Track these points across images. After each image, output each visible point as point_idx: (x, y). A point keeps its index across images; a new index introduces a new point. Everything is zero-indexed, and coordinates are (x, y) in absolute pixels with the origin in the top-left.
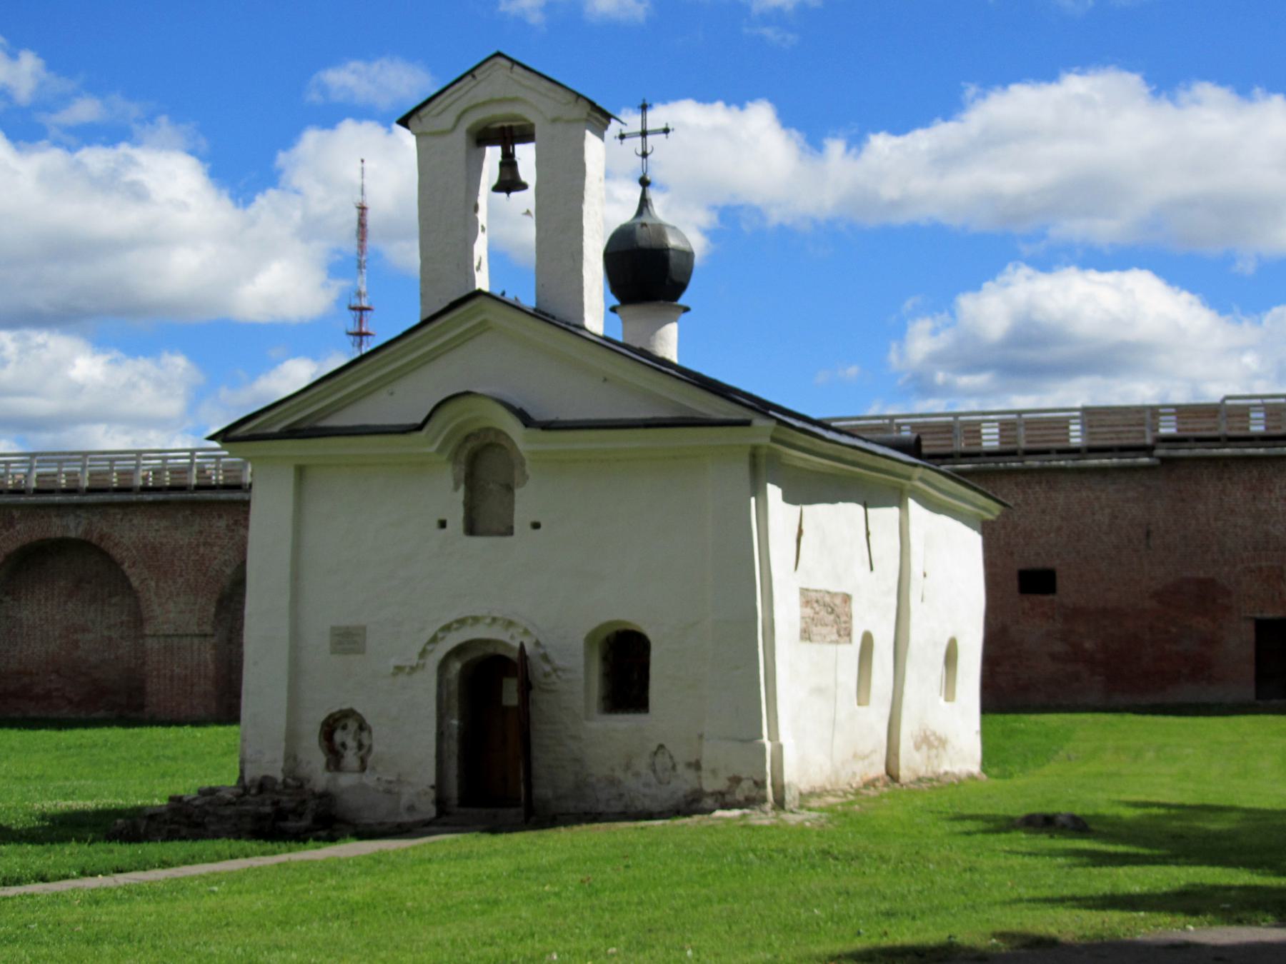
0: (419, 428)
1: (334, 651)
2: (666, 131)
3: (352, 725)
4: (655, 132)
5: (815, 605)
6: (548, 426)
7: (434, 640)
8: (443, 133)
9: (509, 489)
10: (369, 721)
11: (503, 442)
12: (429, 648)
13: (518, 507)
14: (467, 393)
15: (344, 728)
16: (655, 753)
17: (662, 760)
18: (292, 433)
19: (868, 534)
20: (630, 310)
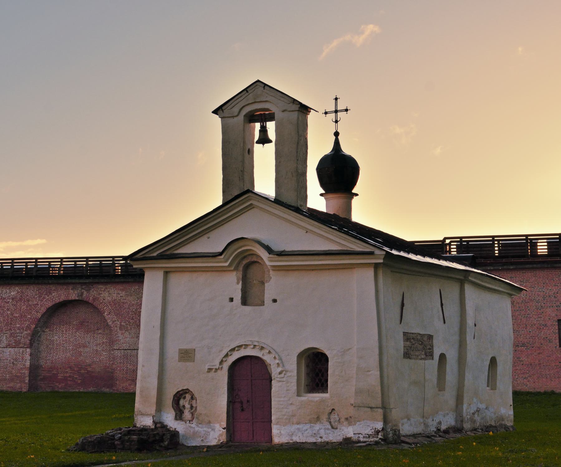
0: (221, 254)
1: (180, 361)
2: (346, 110)
4: (341, 111)
5: (412, 340)
6: (281, 254)
7: (227, 355)
9: (263, 283)
10: (196, 395)
11: (260, 261)
12: (224, 359)
13: (266, 292)
14: (242, 238)
15: (185, 398)
16: (331, 413)
18: (162, 257)
19: (442, 305)
20: (330, 196)
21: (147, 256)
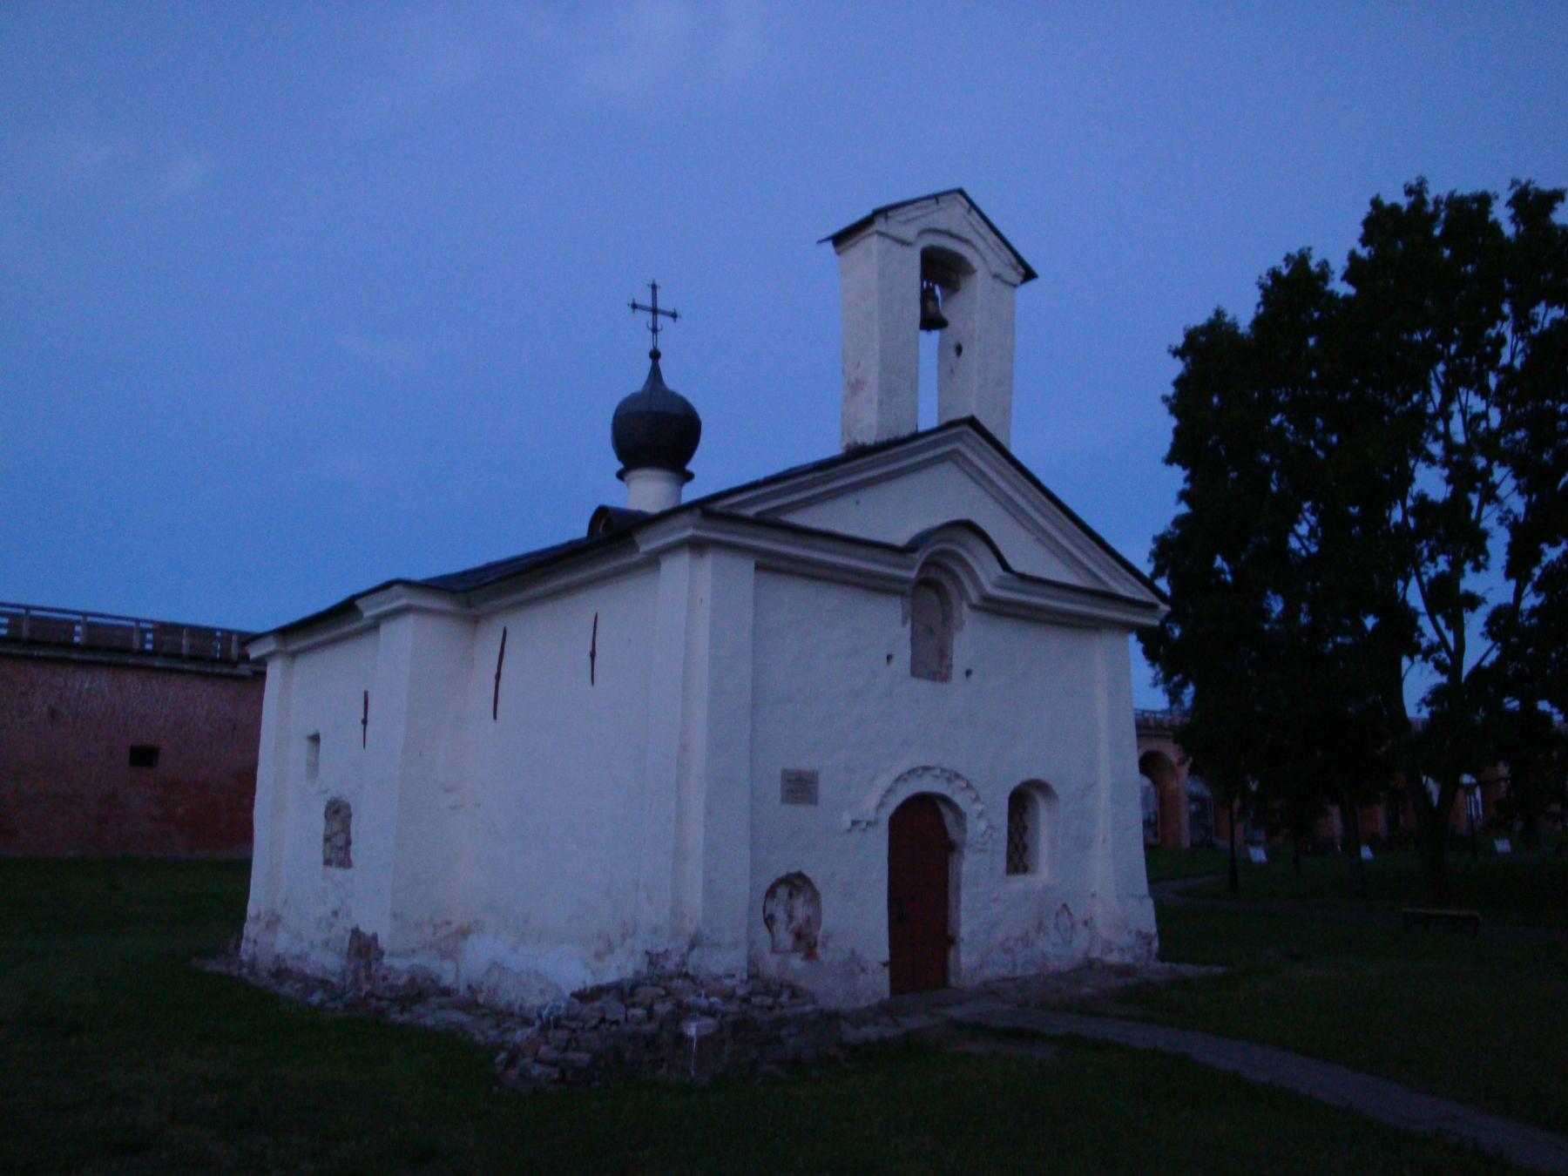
1: (785, 800)
3: (782, 892)
7: (890, 790)
8: (903, 243)
17: (1064, 920)
18: (765, 523)
21: (736, 511)
